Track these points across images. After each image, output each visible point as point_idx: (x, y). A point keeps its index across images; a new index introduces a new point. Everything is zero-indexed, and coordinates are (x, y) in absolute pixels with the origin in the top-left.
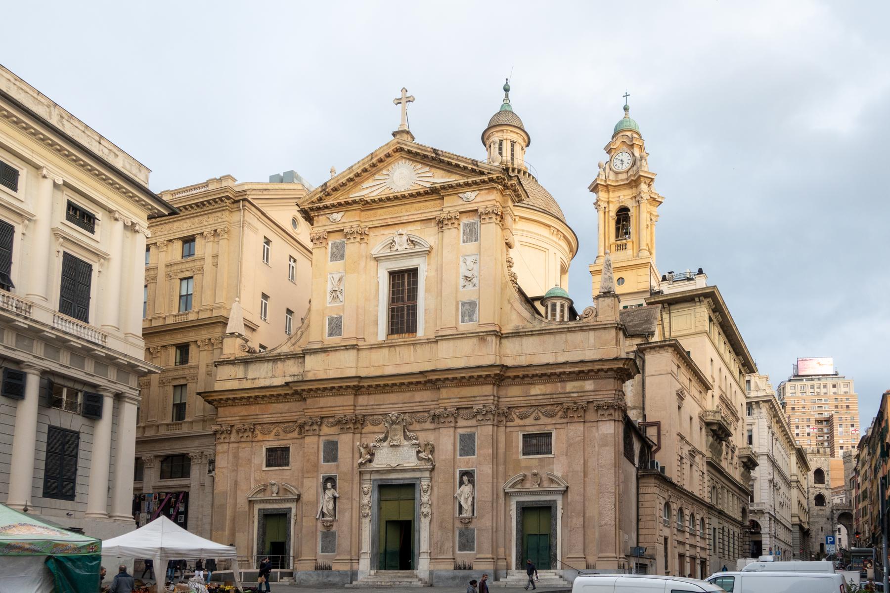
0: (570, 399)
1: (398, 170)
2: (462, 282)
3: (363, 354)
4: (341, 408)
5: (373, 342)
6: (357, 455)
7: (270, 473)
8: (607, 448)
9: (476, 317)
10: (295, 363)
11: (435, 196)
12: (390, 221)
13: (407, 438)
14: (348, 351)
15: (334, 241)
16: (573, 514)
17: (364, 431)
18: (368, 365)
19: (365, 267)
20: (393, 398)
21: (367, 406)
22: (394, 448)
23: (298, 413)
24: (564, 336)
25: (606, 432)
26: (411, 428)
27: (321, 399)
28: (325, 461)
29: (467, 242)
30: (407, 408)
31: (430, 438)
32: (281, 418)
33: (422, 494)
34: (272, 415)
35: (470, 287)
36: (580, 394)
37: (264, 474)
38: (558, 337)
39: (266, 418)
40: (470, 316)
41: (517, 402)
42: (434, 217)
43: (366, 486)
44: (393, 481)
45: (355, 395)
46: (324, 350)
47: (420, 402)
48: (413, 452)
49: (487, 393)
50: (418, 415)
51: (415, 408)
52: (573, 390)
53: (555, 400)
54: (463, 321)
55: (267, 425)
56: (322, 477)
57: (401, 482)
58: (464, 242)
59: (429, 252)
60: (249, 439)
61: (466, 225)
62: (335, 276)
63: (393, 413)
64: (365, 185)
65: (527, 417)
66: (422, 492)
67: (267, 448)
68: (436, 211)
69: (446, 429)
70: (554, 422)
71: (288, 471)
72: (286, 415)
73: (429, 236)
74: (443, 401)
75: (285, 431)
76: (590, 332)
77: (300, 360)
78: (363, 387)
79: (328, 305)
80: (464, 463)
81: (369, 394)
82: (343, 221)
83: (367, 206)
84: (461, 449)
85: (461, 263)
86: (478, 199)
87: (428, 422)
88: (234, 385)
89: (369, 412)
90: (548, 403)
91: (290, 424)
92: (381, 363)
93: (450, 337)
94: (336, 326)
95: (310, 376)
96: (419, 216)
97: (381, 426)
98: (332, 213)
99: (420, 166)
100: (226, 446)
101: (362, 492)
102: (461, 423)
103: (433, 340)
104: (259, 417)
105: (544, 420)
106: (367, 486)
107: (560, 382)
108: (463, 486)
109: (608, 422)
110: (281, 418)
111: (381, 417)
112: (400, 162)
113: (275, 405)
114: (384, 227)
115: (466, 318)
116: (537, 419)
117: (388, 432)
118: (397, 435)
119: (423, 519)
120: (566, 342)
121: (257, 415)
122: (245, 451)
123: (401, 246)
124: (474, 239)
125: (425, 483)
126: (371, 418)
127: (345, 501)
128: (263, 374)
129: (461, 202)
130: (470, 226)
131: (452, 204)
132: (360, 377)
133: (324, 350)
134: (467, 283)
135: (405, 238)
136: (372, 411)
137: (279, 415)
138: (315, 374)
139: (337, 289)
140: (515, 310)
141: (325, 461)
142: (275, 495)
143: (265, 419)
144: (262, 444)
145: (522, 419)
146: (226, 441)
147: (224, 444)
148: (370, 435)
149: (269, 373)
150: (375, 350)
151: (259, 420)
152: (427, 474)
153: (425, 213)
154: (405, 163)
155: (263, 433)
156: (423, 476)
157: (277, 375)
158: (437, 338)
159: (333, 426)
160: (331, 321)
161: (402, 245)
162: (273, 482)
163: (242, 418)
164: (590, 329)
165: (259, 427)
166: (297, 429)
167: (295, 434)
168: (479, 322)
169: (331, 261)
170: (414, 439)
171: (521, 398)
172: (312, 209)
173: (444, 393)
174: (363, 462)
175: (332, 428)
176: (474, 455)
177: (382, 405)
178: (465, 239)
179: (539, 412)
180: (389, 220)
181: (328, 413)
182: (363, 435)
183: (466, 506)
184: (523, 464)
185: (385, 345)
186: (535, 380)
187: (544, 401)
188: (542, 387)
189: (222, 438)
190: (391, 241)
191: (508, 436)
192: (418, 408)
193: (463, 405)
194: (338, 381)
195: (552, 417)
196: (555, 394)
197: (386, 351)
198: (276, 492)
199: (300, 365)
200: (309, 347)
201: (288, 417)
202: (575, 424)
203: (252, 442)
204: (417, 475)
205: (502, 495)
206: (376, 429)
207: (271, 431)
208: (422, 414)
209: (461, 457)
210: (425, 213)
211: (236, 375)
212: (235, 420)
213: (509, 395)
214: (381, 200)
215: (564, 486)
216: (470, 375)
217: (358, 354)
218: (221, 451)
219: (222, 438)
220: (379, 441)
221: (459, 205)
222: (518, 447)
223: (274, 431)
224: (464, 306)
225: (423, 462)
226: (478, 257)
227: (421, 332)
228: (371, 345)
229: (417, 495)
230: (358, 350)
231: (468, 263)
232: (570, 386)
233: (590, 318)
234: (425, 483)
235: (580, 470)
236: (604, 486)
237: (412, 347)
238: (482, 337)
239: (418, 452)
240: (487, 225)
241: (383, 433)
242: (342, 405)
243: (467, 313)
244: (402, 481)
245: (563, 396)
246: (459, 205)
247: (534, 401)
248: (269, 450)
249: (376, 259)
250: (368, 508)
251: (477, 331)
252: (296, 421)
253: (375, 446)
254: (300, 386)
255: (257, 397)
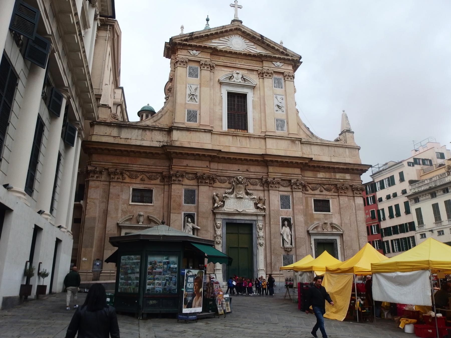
0: (339, 182)
1: (234, 39)
2: (277, 108)
3: (215, 136)
4: (201, 169)
5: (221, 131)
6: (211, 201)
7: (136, 207)
8: (361, 211)
9: (285, 128)
10: (160, 133)
11: (258, 59)
12: (229, 65)
13: (247, 194)
14: (206, 133)
15: (191, 66)
16: (347, 248)
17: (214, 185)
18: (218, 144)
19: (213, 85)
20: (236, 167)
21: (218, 169)
22: (239, 200)
23: (163, 167)
24: (333, 148)
25: (359, 203)
26: (247, 188)
27: (184, 160)
28: (185, 203)
29: (276, 87)
30: (247, 174)
31: (261, 195)
32: (147, 169)
33: (259, 230)
34: (141, 166)
35: (280, 112)
36: (344, 181)
37: (130, 207)
38: (330, 148)
39: (135, 167)
40: (282, 128)
41: (310, 181)
42: (257, 69)
43: (219, 222)
44: (237, 221)
45: (210, 162)
46: (188, 129)
47: (254, 172)
48: (252, 204)
49: (297, 173)
50: (252, 180)
51: (250, 175)
52: (340, 178)
53: (331, 182)
54: (278, 130)
55: (135, 173)
56: (183, 214)
57: (243, 222)
58: (275, 87)
59: (254, 88)
60: (119, 180)
61: (275, 79)
62: (192, 86)
63: (240, 177)
64: (213, 41)
65: (316, 190)
66: (258, 229)
67: (133, 189)
68: (258, 67)
69: (274, 191)
70: (331, 194)
71: (152, 207)
72: (152, 167)
73: (254, 79)
74: (271, 174)
75: (150, 178)
76: (346, 149)
77: (164, 133)
78: (219, 157)
79: (187, 102)
80: (286, 213)
81: (219, 163)
82: (199, 56)
83: (215, 52)
84: (281, 204)
85: (274, 98)
86: (283, 67)
87: (259, 185)
88: (111, 140)
89: (219, 174)
90: (328, 183)
91: (154, 174)
92: (227, 145)
93: (275, 137)
94: (192, 116)
95: (177, 144)
96: (248, 67)
97: (227, 183)
98: (193, 50)
99: (248, 41)
100: (98, 183)
101: (215, 227)
102: (282, 188)
103: (262, 137)
104: (129, 165)
105: (325, 192)
106: (219, 222)
107: (333, 172)
108: (284, 227)
109: (359, 197)
110: (147, 169)
111: (226, 178)
112: (236, 36)
113: (142, 159)
114: (224, 67)
115: (280, 128)
116: (321, 191)
117: (234, 189)
118: (241, 191)
119: (259, 247)
120: (335, 151)
121: (128, 164)
122: (115, 189)
123: (237, 79)
124: (280, 87)
125: (261, 224)
126: (218, 178)
127: (203, 232)
128: (133, 138)
129: (273, 66)
130: (279, 80)
131: (267, 66)
132: (220, 151)
133: (188, 129)
134: (278, 109)
135: (240, 76)
136: (221, 173)
137: (147, 167)
138: (181, 143)
139: (194, 94)
140: (302, 129)
141: (185, 203)
142: (141, 223)
143: (134, 168)
144: (129, 185)
145: (313, 190)
146: (99, 179)
147: (96, 181)
148: (218, 189)
149: (139, 137)
150: (222, 136)
151: (129, 168)
152: (261, 218)
153: (251, 66)
154: (239, 37)
155: (131, 177)
156: (258, 219)
157: (145, 139)
158: (267, 136)
159: (192, 180)
160: (189, 112)
161: (237, 79)
162: (142, 213)
163: (114, 164)
164: (346, 147)
165: (128, 173)
166: (159, 178)
167: (158, 181)
168: (288, 131)
169: (189, 77)
170: (253, 195)
171: (313, 179)
172: (180, 44)
173: (271, 169)
174: (218, 206)
175: (192, 181)
176: (290, 209)
177: (228, 170)
178: (275, 85)
179: (322, 187)
180: (228, 64)
181: (190, 170)
182: (214, 188)
183: (288, 239)
184: (315, 216)
185: (231, 134)
186: (321, 170)
187: (325, 182)
188: (323, 174)
189: (95, 176)
190: (231, 76)
191: (306, 198)
192: (253, 175)
193: (284, 177)
194: (203, 151)
195: (329, 191)
196: (332, 179)
197: (230, 138)
198: (142, 221)
199: (164, 135)
200: (175, 125)
201: (153, 168)
202: (343, 196)
203: (121, 182)
204: (254, 218)
205: (306, 234)
206: (223, 185)
207: (138, 177)
208: (254, 180)
209: (282, 209)
210: (251, 66)
211: (111, 134)
212: (108, 165)
213: (306, 175)
214: (226, 52)
215: (342, 231)
216: (291, 161)
217: (211, 136)
218: (94, 186)
219: (95, 176)
220: (229, 193)
221: (273, 67)
222: (312, 206)
223: (141, 177)
224: (277, 121)
225: (258, 210)
226: (284, 97)
227: (251, 130)
228: (221, 132)
229: (254, 231)
230: (212, 133)
231: (279, 99)
232: (338, 176)
233: (342, 141)
234: (260, 224)
235: (348, 222)
236: (361, 232)
237: (248, 138)
238: (293, 141)
239: (256, 204)
240: (289, 82)
241: (230, 188)
242: (201, 166)
243: (280, 125)
244: (244, 221)
245: (336, 180)
246: (273, 67)
247: (320, 181)
248: (134, 190)
249: (221, 83)
250: (219, 237)
251: (290, 136)
252: (162, 173)
253: (226, 197)
254: (174, 149)
255: (131, 151)
